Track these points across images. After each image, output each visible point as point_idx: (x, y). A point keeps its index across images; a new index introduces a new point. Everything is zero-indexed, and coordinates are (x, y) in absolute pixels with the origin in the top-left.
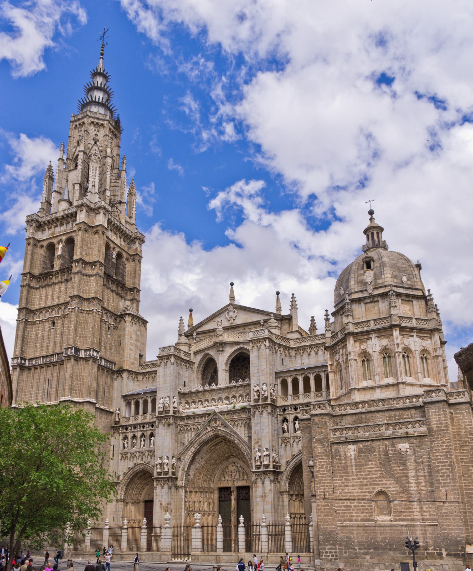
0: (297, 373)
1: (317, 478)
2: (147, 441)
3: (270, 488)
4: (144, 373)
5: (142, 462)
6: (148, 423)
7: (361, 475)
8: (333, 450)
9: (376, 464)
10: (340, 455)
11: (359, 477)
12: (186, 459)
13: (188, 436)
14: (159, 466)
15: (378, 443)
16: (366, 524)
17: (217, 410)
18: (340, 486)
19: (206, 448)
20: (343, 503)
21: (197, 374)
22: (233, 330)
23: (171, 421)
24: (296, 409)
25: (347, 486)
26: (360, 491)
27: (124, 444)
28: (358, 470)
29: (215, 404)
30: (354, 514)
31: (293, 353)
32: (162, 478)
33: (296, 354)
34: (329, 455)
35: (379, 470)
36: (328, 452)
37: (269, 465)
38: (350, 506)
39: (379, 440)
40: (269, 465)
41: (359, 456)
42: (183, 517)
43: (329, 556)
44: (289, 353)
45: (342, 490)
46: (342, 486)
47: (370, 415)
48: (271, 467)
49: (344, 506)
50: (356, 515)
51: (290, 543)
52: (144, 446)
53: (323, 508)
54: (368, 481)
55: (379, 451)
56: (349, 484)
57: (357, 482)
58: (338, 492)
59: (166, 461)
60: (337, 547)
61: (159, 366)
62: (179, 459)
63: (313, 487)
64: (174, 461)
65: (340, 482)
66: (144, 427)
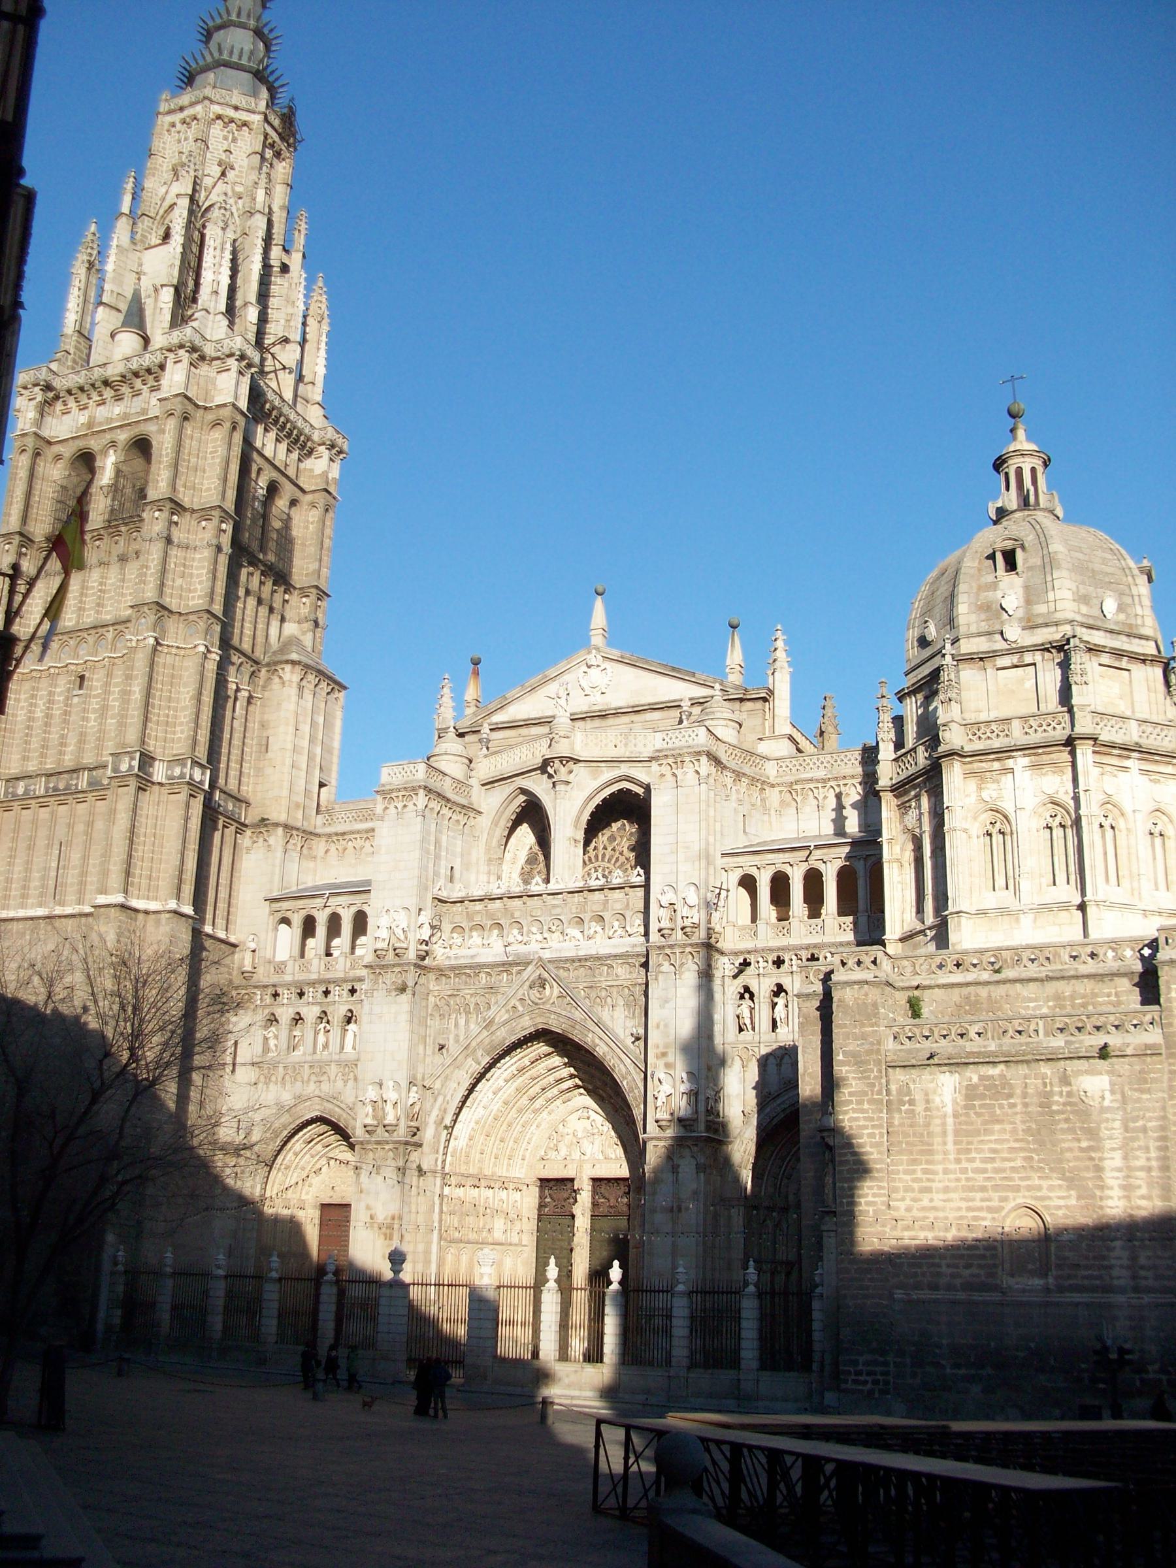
0: (787, 857)
1: (842, 1163)
2: (335, 1032)
3: (694, 1186)
4: (330, 835)
5: (317, 1093)
6: (337, 982)
7: (972, 1160)
9: (1014, 1131)
10: (912, 1102)
11: (964, 1164)
13: (456, 1025)
14: (369, 1109)
15: (1023, 1070)
16: (977, 1297)
17: (547, 955)
18: (907, 1189)
19: (509, 1065)
21: (488, 850)
22: (597, 723)
23: (411, 978)
24: (779, 963)
25: (928, 1190)
26: (964, 1205)
27: (266, 1039)
28: (964, 1146)
29: (540, 937)
30: (944, 1269)
31: (773, 796)
32: (378, 1143)
33: (782, 802)
34: (880, 1101)
35: (1022, 1149)
36: (880, 1093)
37: (696, 1120)
39: (1027, 1062)
40: (696, 1120)
41: (966, 1107)
42: (434, 1258)
43: (866, 1382)
44: (763, 800)
45: (914, 1200)
46: (913, 1190)
47: (1001, 990)
48: (702, 1127)
50: (950, 1270)
51: (756, 1344)
52: (326, 1046)
55: (1025, 1095)
56: (934, 1185)
57: (958, 1180)
58: (902, 1205)
60: (890, 1358)
61: (382, 819)
63: (828, 1190)
64: (414, 1096)
65: (908, 1177)
66: (326, 993)
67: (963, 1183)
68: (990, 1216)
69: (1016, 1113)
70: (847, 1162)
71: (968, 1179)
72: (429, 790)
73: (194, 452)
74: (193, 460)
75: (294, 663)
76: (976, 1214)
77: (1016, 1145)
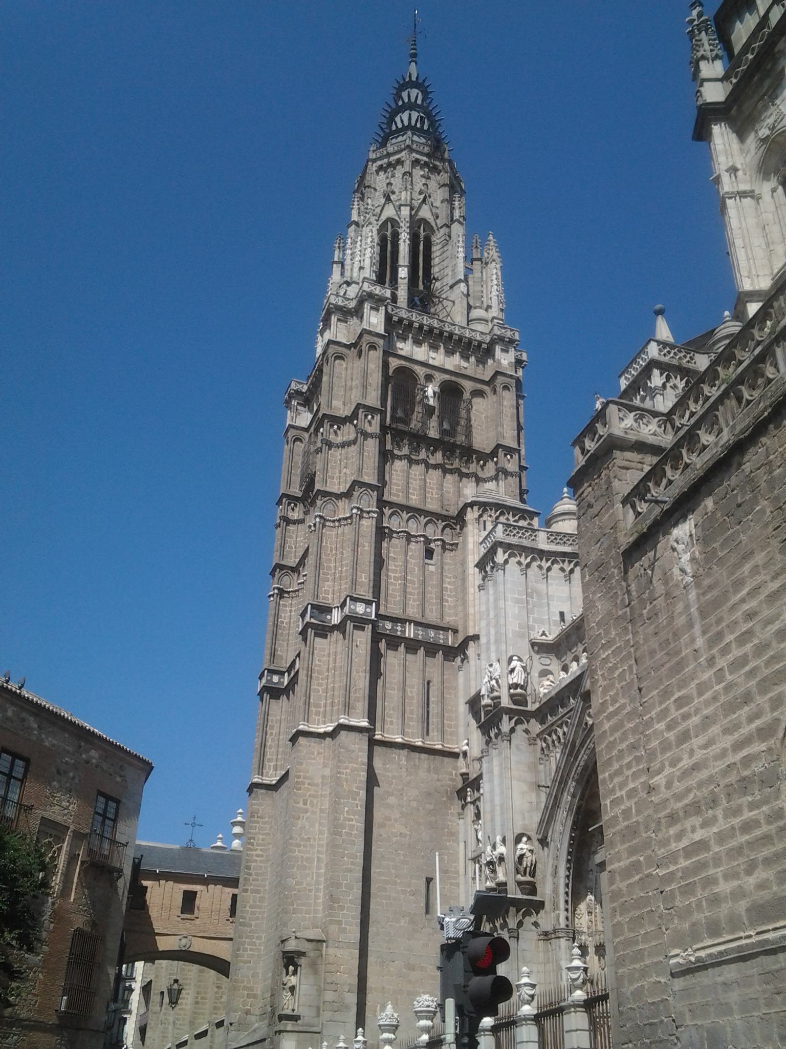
7: (725, 651)
8: (633, 587)
12: (556, 836)
18: (666, 746)
20: (679, 836)
25: (685, 736)
30: (724, 887)
38: (702, 845)
41: (707, 560)
45: (674, 763)
49: (688, 852)
53: (623, 885)
54: (752, 673)
57: (715, 698)
58: (659, 780)
59: (501, 849)
62: (543, 842)
65: (661, 726)
67: (723, 699)
68: (763, 747)
69: (767, 525)
70: (605, 732)
71: (727, 689)
72: (508, 547)
73: (349, 378)
74: (349, 383)
75: (472, 505)
76: (744, 753)
77: (775, 585)
